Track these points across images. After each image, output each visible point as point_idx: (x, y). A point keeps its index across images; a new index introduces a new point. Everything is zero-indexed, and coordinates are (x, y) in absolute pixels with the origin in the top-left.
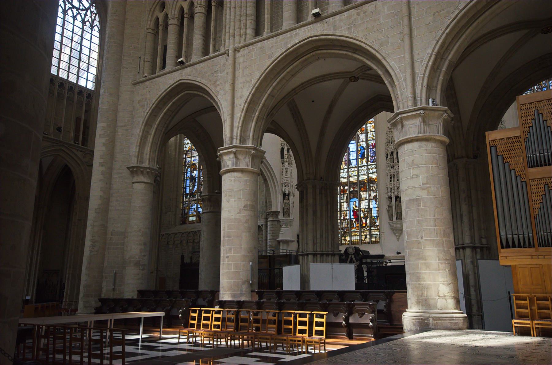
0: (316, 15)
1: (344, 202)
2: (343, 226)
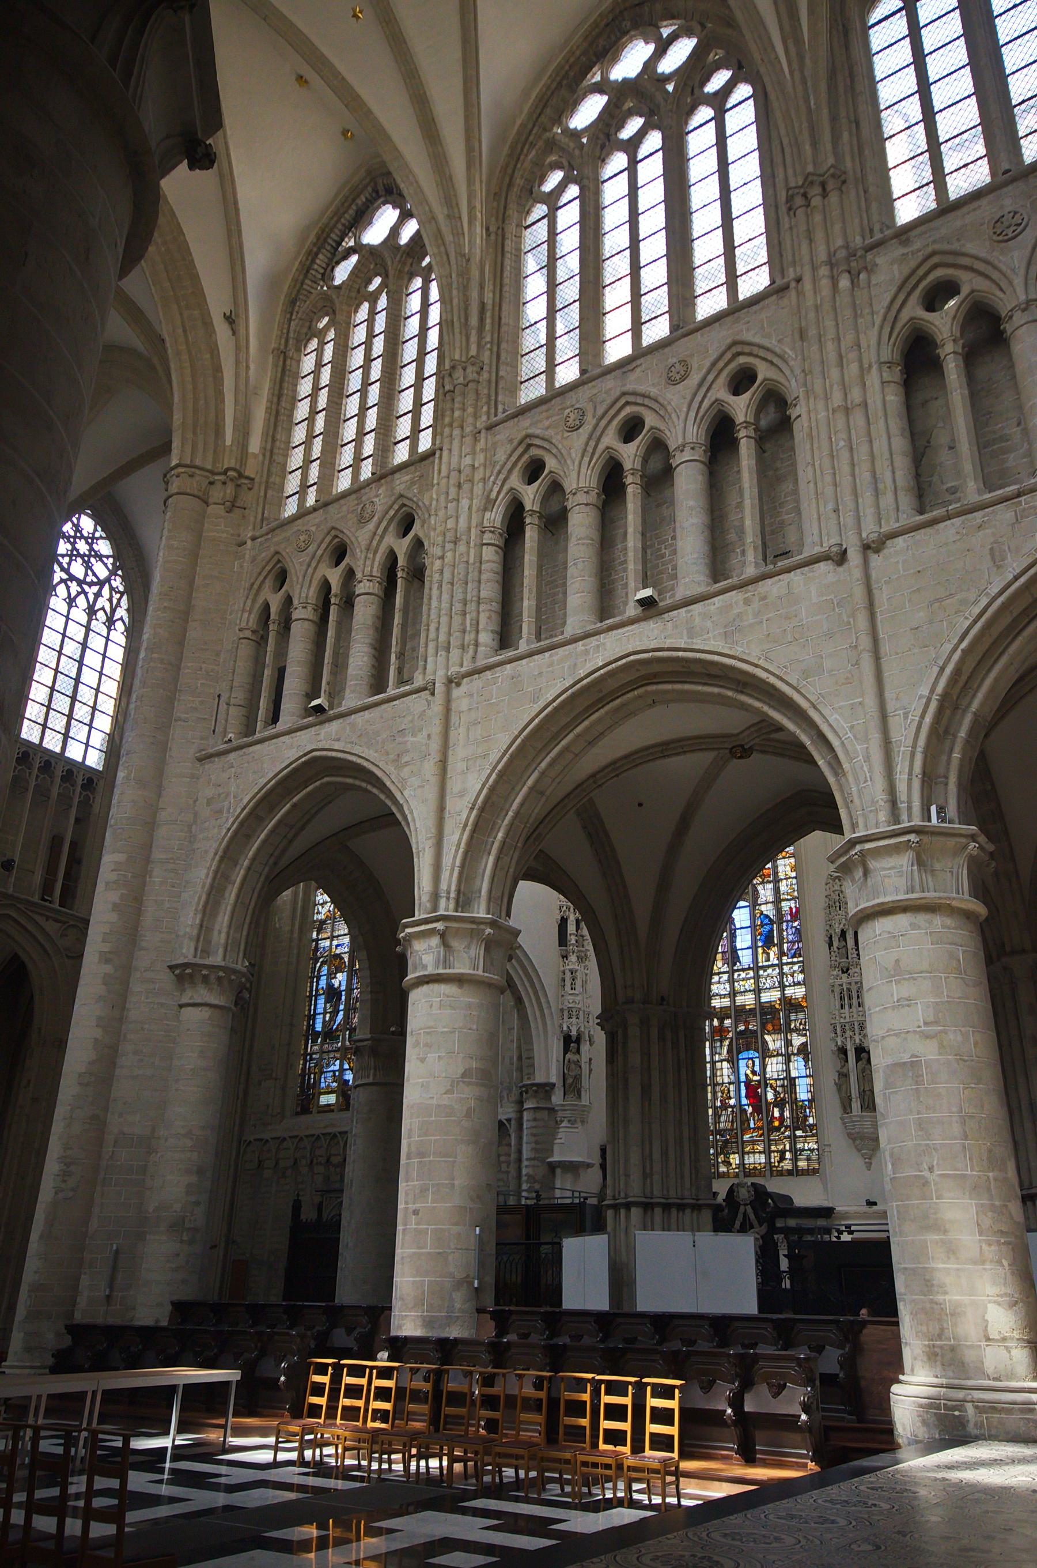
0: (647, 603)
1: (721, 1061)
2: (722, 1125)
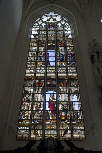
1: (38, 94)
